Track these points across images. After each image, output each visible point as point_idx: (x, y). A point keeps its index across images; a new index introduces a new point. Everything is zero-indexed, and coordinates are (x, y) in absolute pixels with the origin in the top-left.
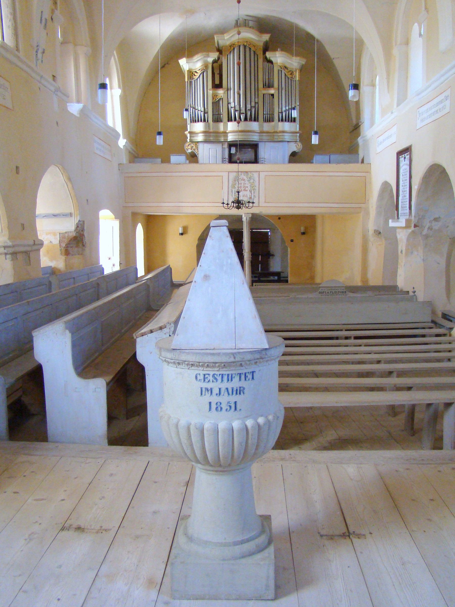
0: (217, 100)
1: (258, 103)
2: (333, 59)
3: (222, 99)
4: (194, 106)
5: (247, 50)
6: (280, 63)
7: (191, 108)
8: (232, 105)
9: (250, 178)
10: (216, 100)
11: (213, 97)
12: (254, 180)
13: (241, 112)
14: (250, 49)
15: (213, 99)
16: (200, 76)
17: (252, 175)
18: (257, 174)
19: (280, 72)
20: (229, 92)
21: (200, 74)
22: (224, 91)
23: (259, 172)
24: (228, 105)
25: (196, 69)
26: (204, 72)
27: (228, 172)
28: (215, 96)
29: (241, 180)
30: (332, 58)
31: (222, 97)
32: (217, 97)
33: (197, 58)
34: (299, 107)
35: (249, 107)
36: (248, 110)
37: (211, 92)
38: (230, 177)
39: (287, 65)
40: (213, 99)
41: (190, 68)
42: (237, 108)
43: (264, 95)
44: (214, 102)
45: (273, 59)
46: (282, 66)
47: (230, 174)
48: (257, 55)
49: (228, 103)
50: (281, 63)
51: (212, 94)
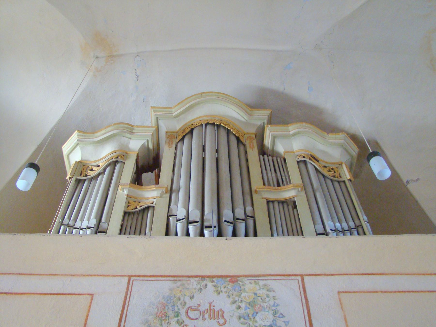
0: (139, 208)
1: (253, 217)
2: (408, 182)
3: (154, 207)
4: (71, 223)
5: (223, 134)
6: (298, 151)
7: (62, 227)
8: (181, 213)
9: (252, 304)
10: (136, 208)
11: (129, 203)
12: (275, 313)
13: (206, 224)
14: (228, 132)
15: (128, 206)
16: (105, 170)
17: (263, 292)
18: (294, 284)
19: (302, 166)
20: (174, 195)
21: (107, 166)
22: (160, 192)
23: (302, 276)
24: (168, 220)
25: (97, 161)
26: (115, 163)
27: (130, 277)
28: (135, 202)
29: (203, 314)
30: (405, 180)
31: (154, 204)
32: (141, 204)
33: (105, 133)
34: (370, 225)
35: (227, 214)
36: (225, 221)
37: (126, 192)
38: (134, 301)
39: (318, 155)
40: (128, 206)
41: (83, 159)
42: (195, 215)
43: (268, 202)
44: (129, 213)
45: (280, 148)
46: (305, 154)
47: (137, 285)
48: (244, 145)
49: (168, 216)
50: (303, 150)
51: (128, 196)
